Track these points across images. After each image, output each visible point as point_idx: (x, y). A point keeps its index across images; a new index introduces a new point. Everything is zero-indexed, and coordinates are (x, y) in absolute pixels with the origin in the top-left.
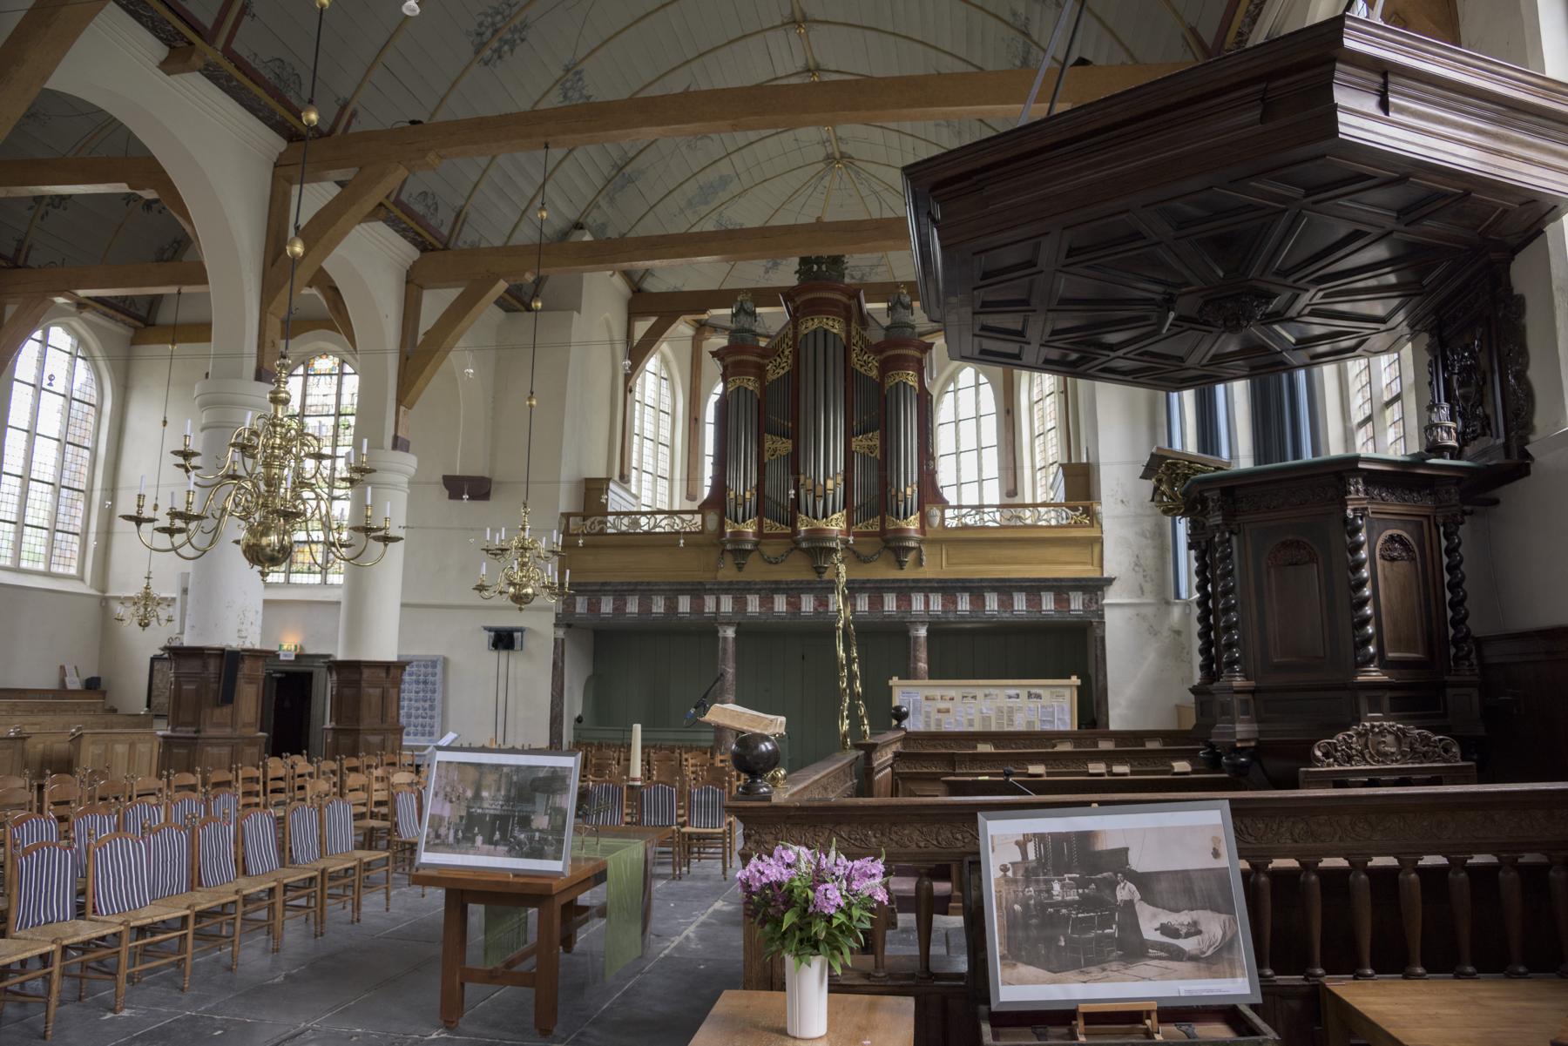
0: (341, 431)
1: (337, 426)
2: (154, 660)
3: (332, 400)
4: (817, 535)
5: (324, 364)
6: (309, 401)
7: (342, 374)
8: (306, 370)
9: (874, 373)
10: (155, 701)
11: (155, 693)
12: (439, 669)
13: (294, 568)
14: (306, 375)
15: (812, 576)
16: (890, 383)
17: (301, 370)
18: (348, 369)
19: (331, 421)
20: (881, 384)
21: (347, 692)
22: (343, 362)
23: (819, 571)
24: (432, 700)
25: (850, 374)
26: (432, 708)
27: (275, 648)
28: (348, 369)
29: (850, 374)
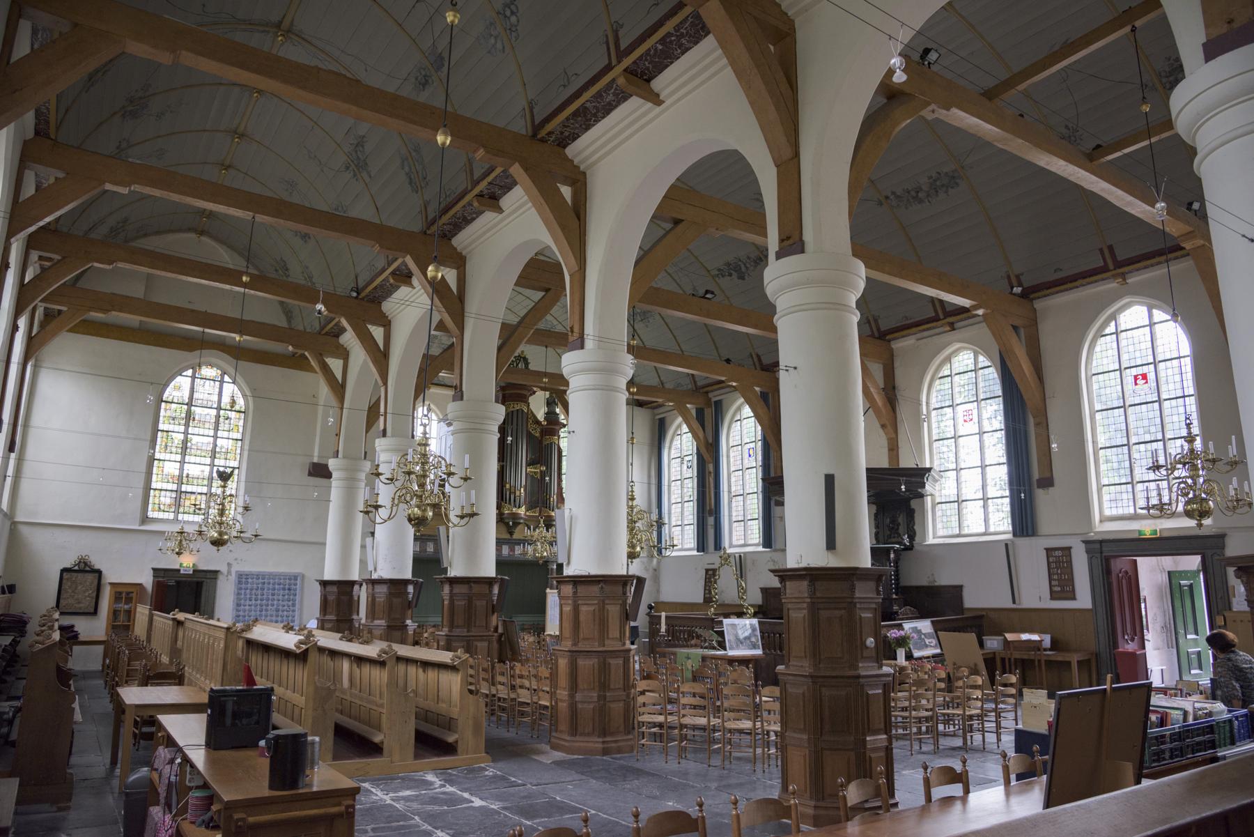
0: (221, 420)
1: (218, 417)
2: (64, 571)
3: (215, 398)
4: (515, 516)
5: (207, 371)
6: (196, 395)
7: (222, 382)
8: (194, 373)
9: (538, 435)
10: (63, 602)
11: (63, 595)
12: (298, 582)
13: (181, 510)
14: (193, 377)
15: (508, 536)
16: (545, 443)
17: (190, 372)
18: (227, 378)
19: (214, 412)
20: (541, 442)
21: (344, 598)
22: (224, 373)
23: (511, 533)
24: (294, 600)
25: (529, 435)
26: (294, 605)
27: (177, 567)
28: (227, 378)
29: (529, 435)
